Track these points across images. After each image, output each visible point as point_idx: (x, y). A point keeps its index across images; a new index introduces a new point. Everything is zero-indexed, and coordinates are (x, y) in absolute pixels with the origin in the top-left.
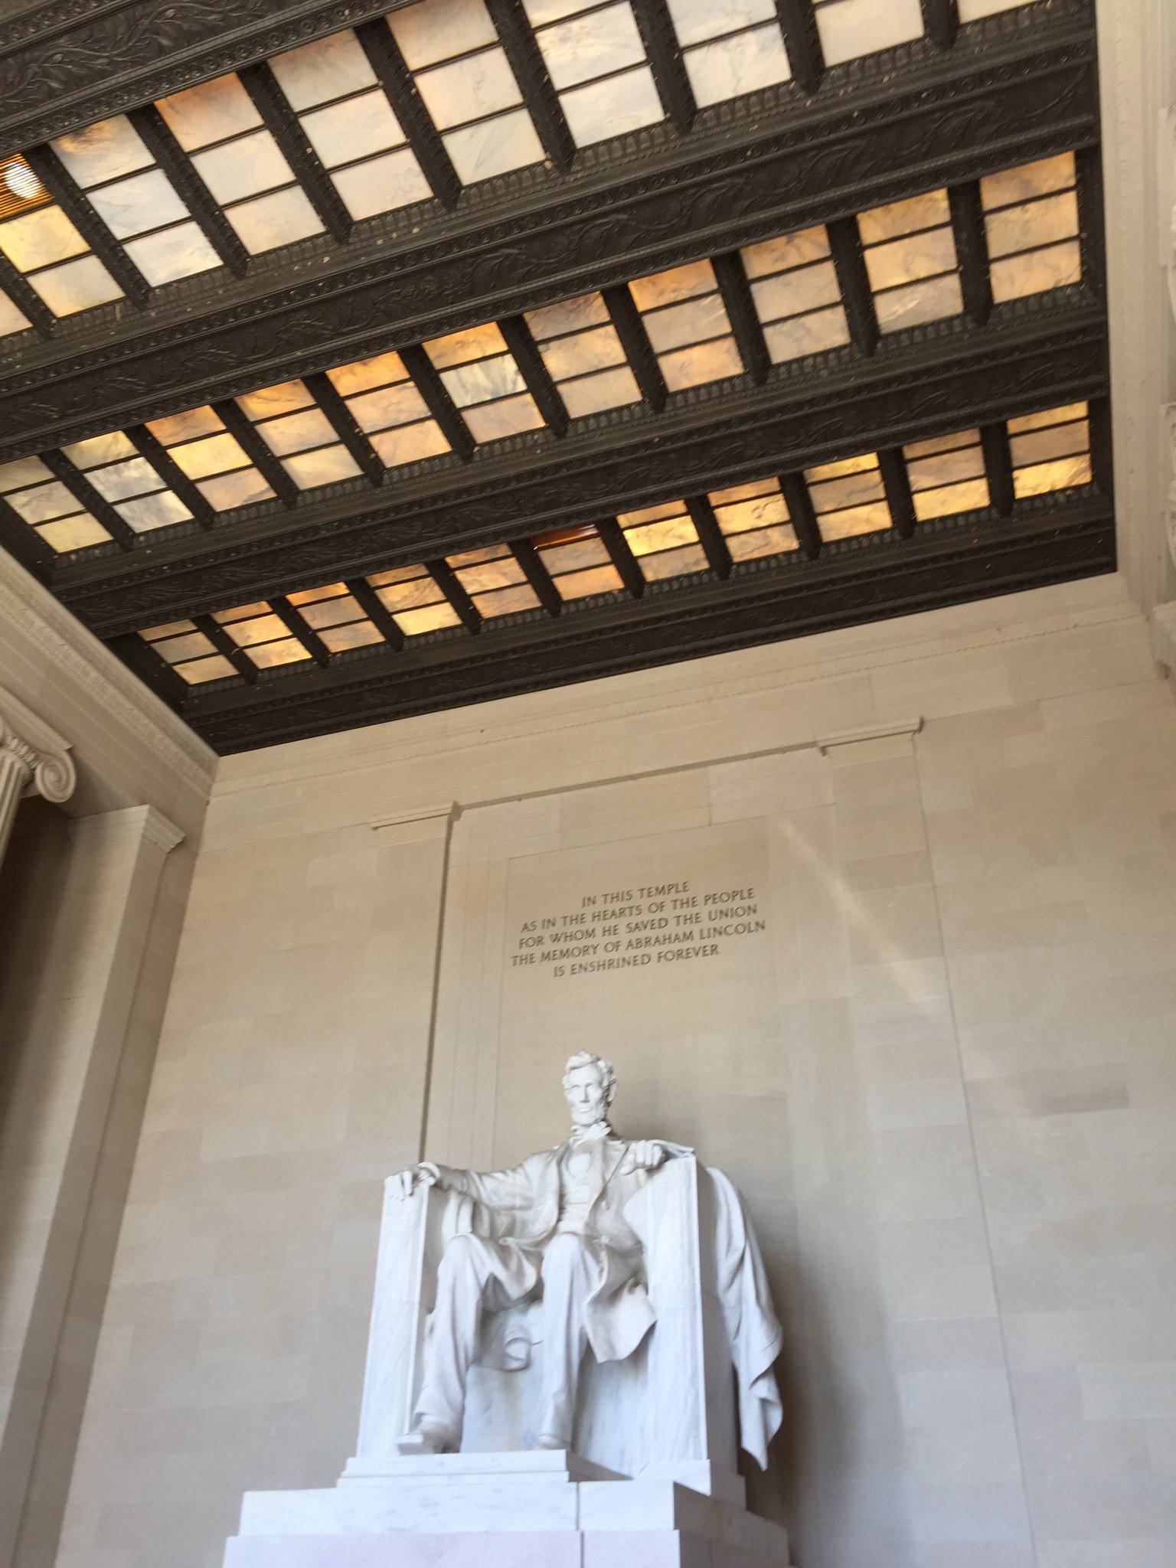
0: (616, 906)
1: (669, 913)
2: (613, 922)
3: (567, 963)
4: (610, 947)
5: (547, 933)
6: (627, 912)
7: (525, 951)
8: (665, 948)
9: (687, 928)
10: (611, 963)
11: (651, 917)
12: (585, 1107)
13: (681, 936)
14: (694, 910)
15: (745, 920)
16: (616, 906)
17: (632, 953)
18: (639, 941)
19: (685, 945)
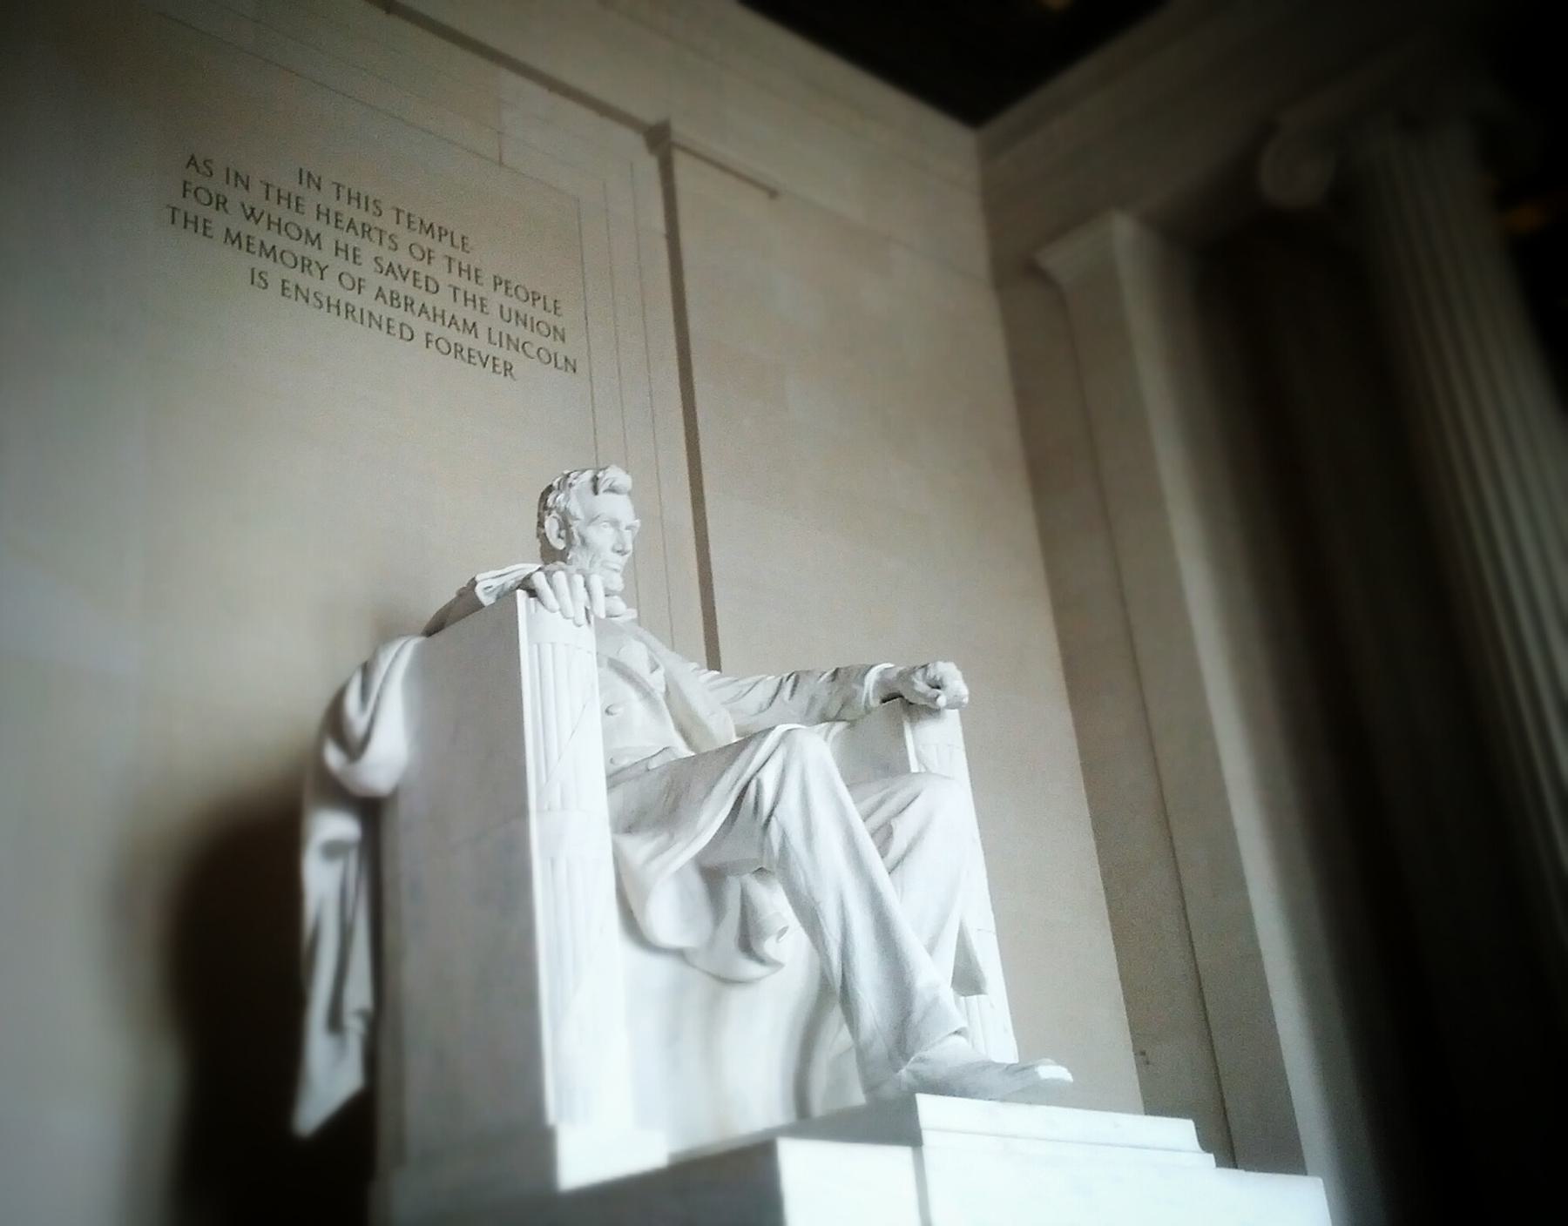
0: (360, 217)
1: (438, 270)
2: (351, 240)
3: (276, 272)
4: (347, 281)
5: (235, 196)
6: (375, 235)
7: (192, 207)
8: (437, 329)
9: (469, 314)
10: (349, 312)
11: (416, 265)
12: (619, 561)
13: (460, 323)
14: (481, 291)
15: (550, 344)
16: (360, 217)
17: (381, 310)
18: (394, 298)
19: (467, 340)
